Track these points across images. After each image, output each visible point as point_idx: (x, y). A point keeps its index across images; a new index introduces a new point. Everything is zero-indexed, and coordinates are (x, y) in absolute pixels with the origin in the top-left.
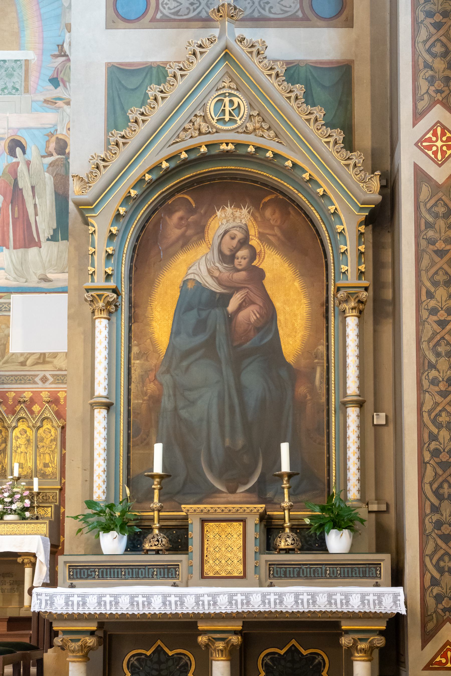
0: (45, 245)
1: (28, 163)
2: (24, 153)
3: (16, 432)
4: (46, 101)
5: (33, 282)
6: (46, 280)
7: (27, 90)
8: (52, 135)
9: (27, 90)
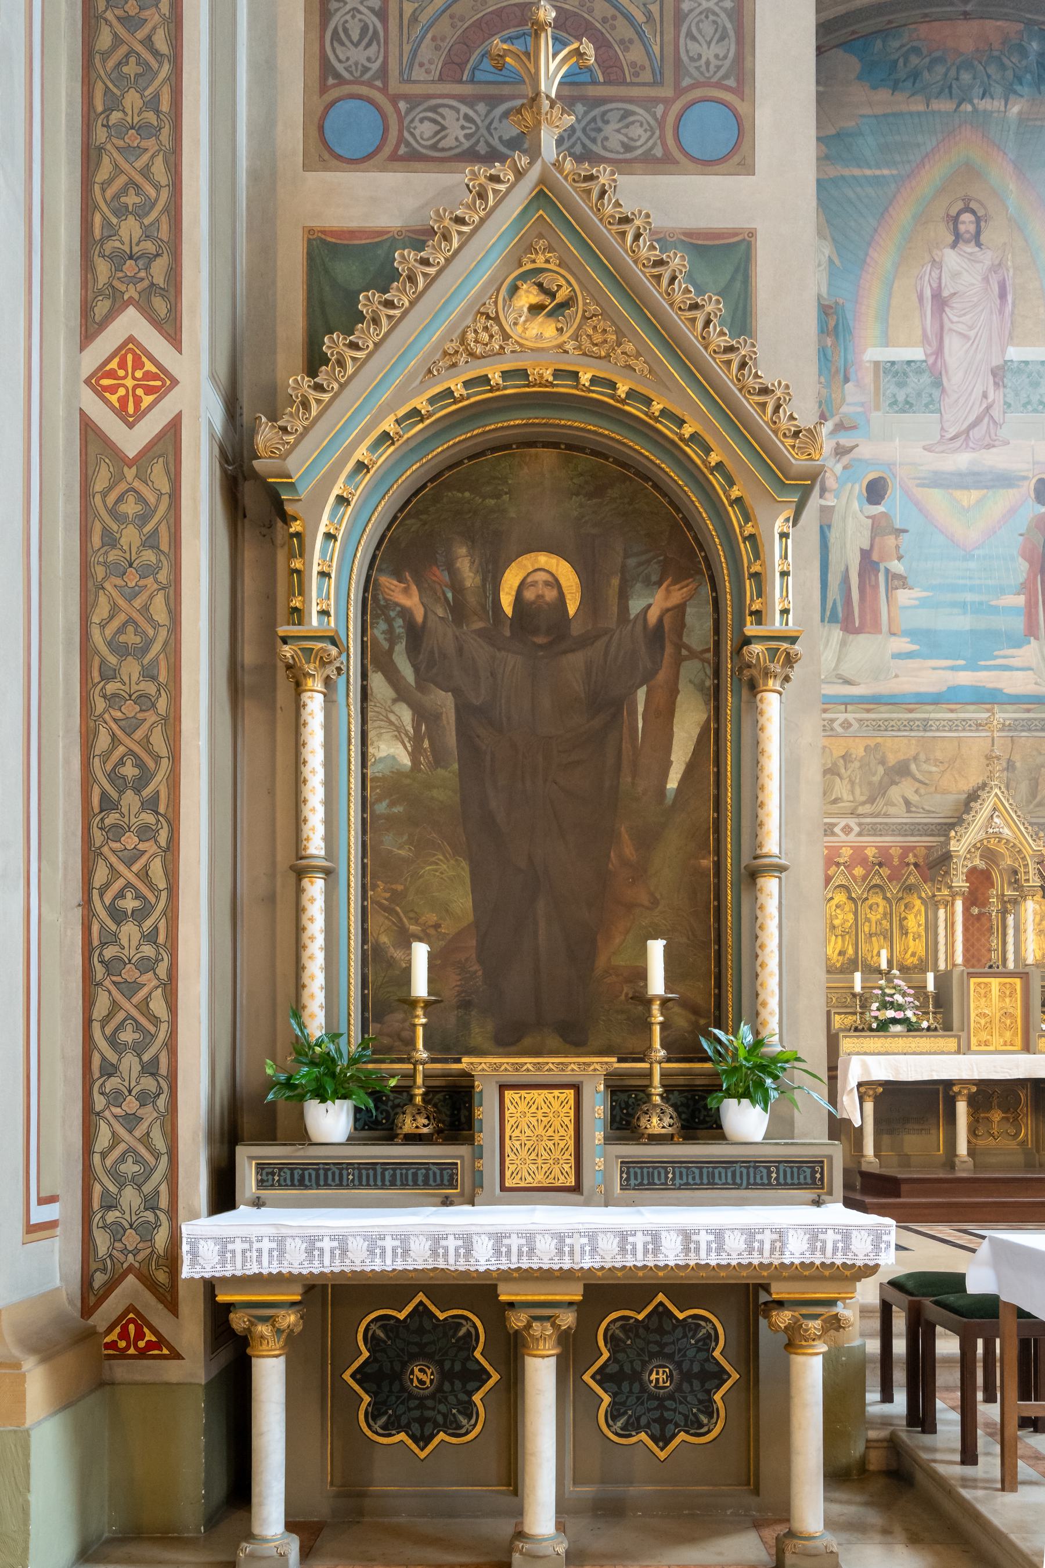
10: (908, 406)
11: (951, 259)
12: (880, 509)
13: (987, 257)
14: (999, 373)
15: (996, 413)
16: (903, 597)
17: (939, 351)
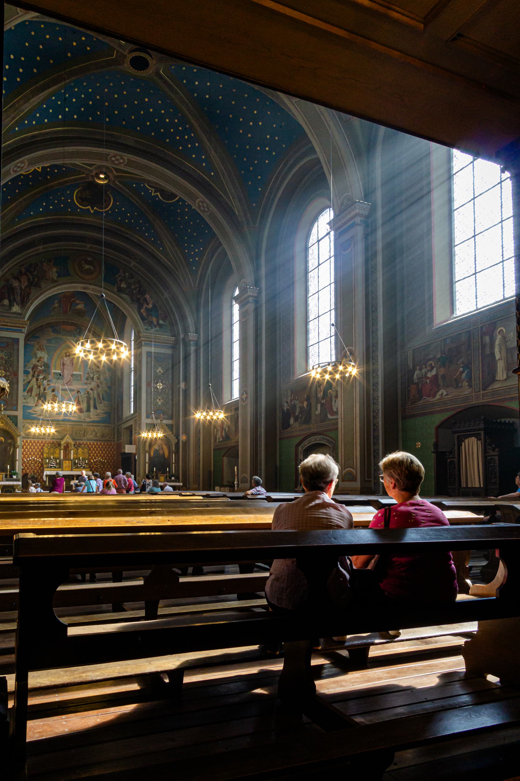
0: (85, 413)
1: (81, 396)
2: (80, 393)
3: (79, 450)
4: (85, 383)
5: (82, 420)
6: (85, 420)
7: (81, 380)
8: (86, 390)
9: (81, 380)
11: (65, 359)
12: (54, 393)
14: (72, 375)
15: (72, 381)
17: (63, 371)
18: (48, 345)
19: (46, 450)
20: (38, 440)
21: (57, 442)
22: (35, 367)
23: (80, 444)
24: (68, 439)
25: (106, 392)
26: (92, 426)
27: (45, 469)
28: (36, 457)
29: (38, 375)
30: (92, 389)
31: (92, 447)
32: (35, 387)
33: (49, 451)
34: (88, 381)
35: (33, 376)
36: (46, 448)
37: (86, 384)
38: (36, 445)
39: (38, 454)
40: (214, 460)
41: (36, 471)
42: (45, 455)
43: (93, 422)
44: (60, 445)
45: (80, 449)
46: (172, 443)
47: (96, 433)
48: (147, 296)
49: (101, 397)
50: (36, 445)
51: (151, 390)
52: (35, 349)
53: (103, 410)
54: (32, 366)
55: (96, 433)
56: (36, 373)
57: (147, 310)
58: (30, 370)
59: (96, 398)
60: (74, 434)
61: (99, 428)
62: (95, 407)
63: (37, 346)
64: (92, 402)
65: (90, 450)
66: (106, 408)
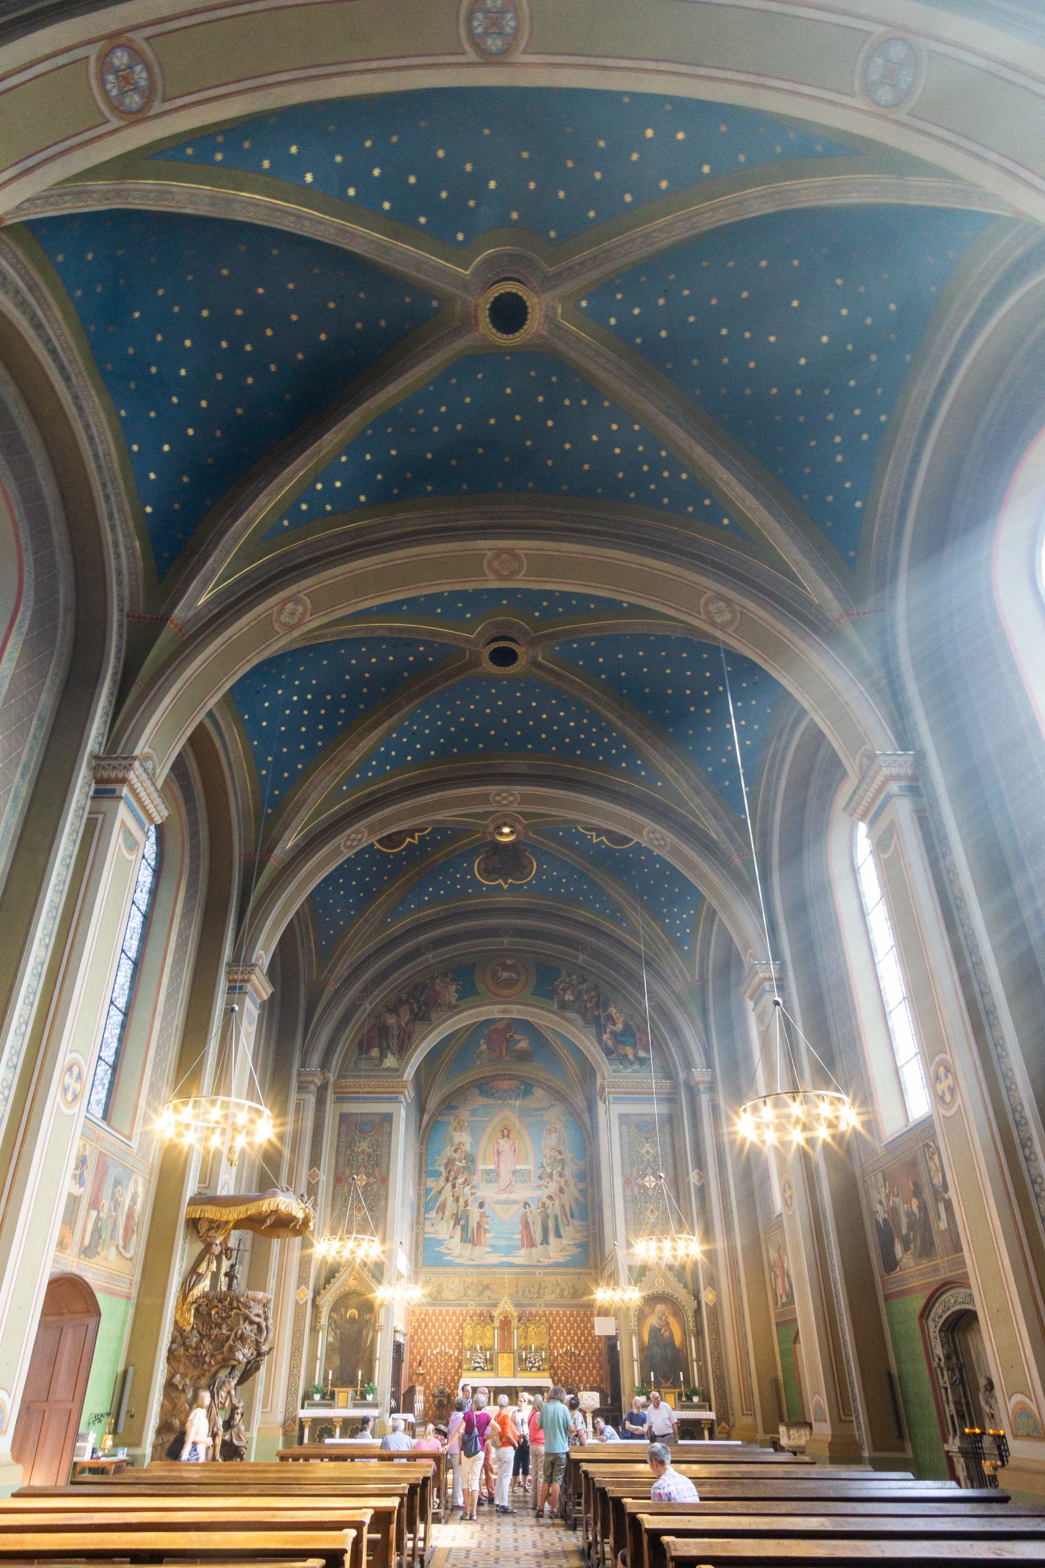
0: (539, 1247)
5: (535, 1263)
10: (490, 1181)
11: (502, 1142)
13: (511, 1141)
14: (514, 1172)
16: (488, 1235)
18: (472, 1119)
19: (468, 1331)
20: (460, 1308)
21: (489, 1312)
22: (450, 1163)
23: (531, 1314)
24: (506, 1306)
25: (576, 1200)
26: (554, 1274)
27: (465, 1374)
28: (450, 1347)
29: (455, 1178)
30: (550, 1198)
31: (554, 1321)
32: (450, 1199)
33: (474, 1334)
34: (543, 1182)
35: (447, 1180)
36: (469, 1326)
37: (539, 1187)
38: (451, 1320)
39: (454, 1339)
40: (780, 1351)
41: (449, 1378)
42: (466, 1342)
43: (557, 1265)
44: (492, 1318)
45: (533, 1326)
46: (686, 1311)
47: (562, 1290)
48: (613, 1011)
49: (568, 1212)
50: (451, 1320)
51: (632, 1191)
52: (451, 1128)
53: (573, 1239)
54: (445, 1161)
55: (562, 1290)
56: (452, 1173)
57: (614, 1034)
58: (442, 1169)
59: (559, 1214)
60: (520, 1293)
61: (567, 1278)
62: (558, 1235)
63: (454, 1124)
64: (551, 1224)
65: (551, 1327)
66: (578, 1235)
